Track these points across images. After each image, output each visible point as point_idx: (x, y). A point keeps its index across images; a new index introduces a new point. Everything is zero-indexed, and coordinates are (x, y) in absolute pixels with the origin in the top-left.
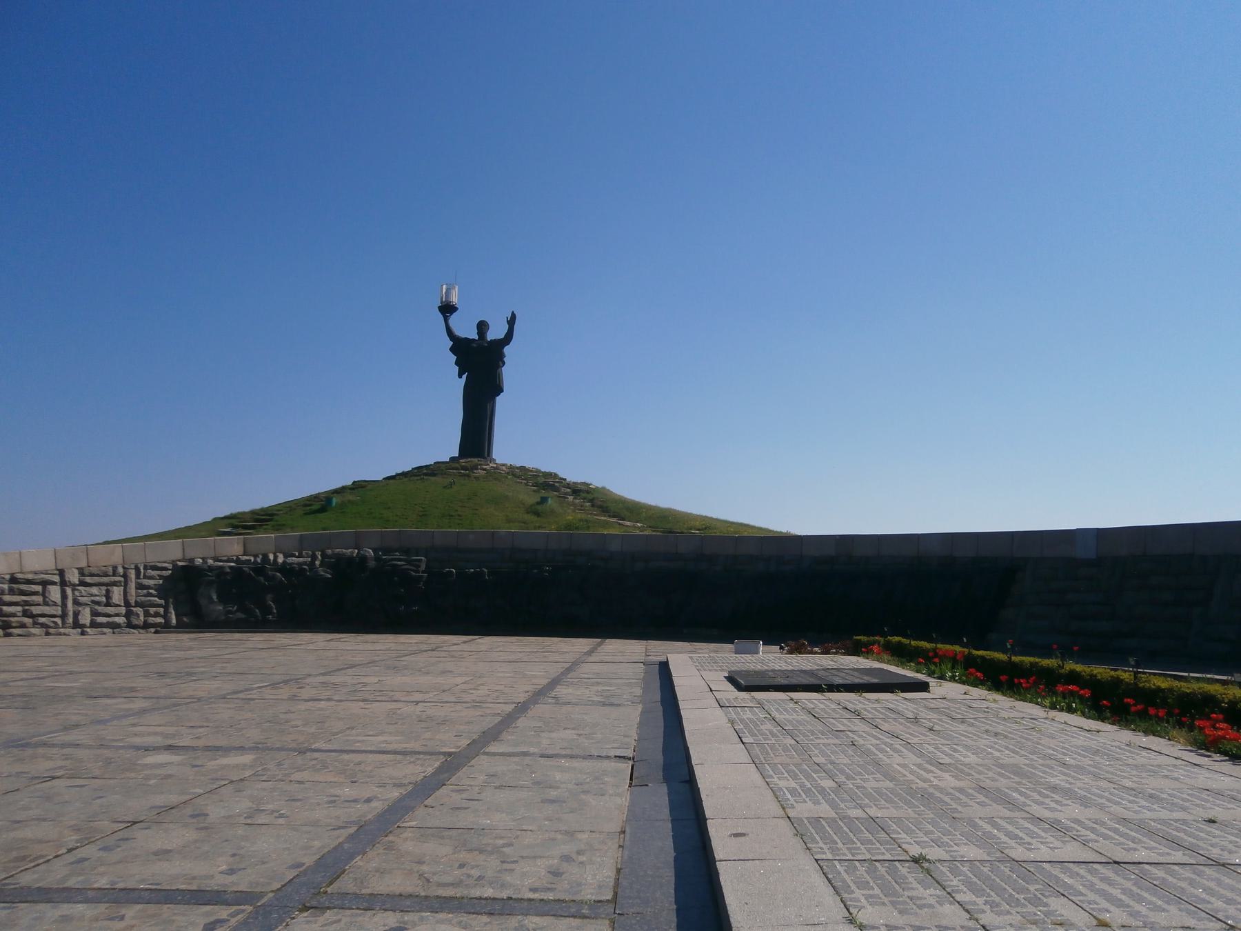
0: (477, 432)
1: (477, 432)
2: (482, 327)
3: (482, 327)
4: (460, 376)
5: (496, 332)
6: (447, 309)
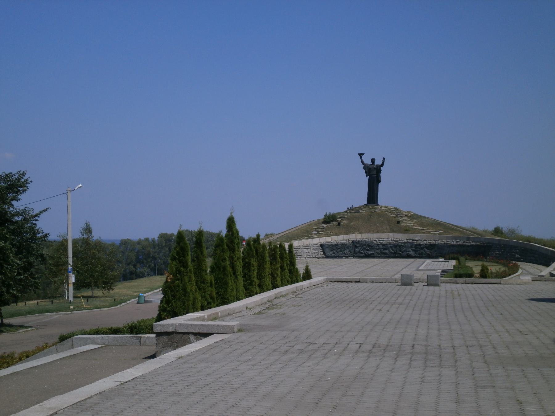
0: (372, 197)
1: (372, 197)
2: (373, 160)
3: (373, 160)
5: (378, 162)
6: (361, 155)
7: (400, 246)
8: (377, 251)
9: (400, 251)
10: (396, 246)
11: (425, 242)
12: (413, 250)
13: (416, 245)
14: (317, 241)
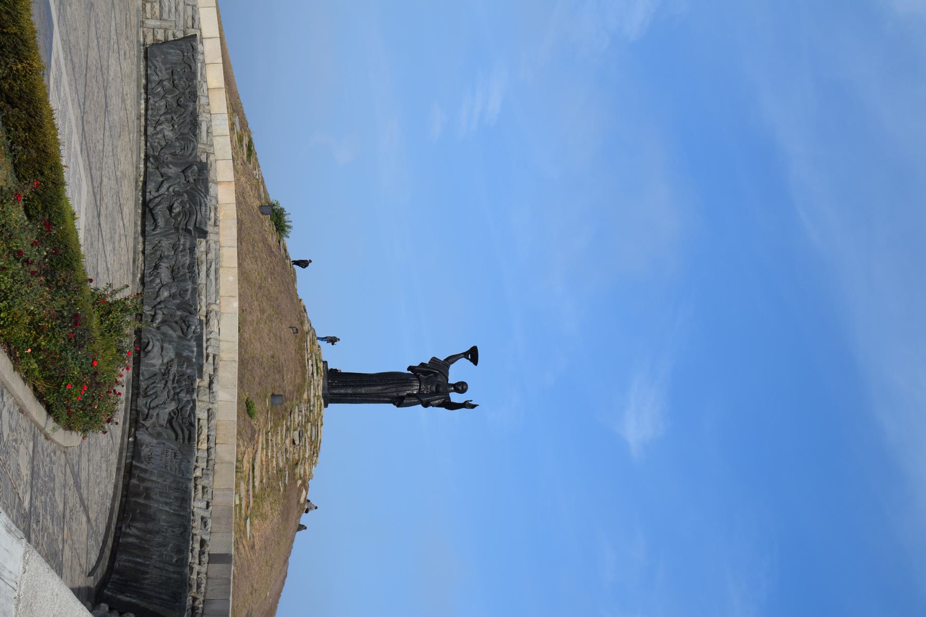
3: (461, 387)
4: (410, 368)
6: (473, 355)
7: (185, 323)
8: (165, 243)
9: (164, 322)
10: (189, 308)
11: (201, 414)
12: (169, 365)
13: (192, 379)
14: (208, 26)
